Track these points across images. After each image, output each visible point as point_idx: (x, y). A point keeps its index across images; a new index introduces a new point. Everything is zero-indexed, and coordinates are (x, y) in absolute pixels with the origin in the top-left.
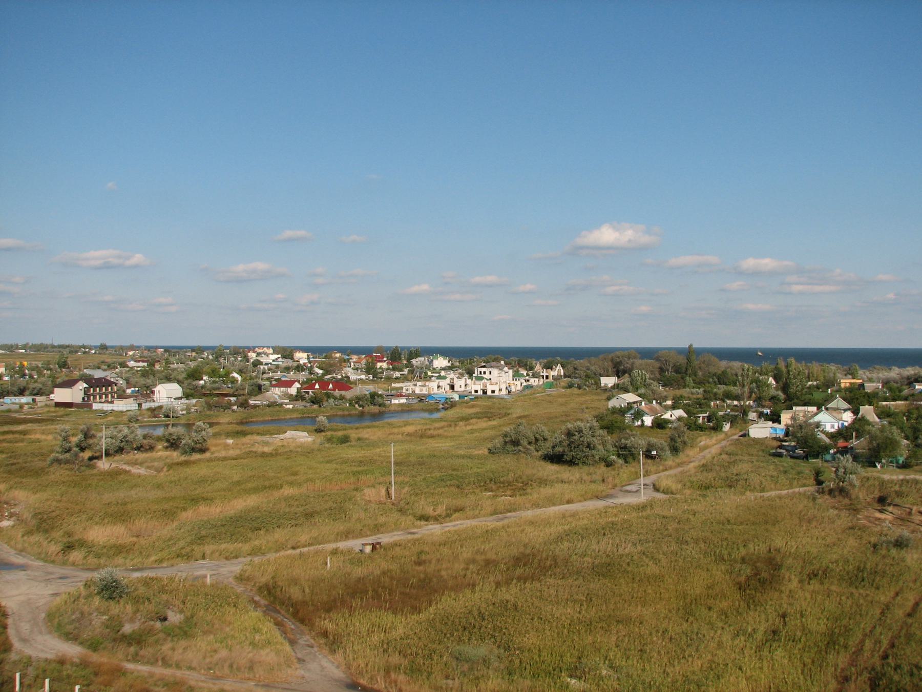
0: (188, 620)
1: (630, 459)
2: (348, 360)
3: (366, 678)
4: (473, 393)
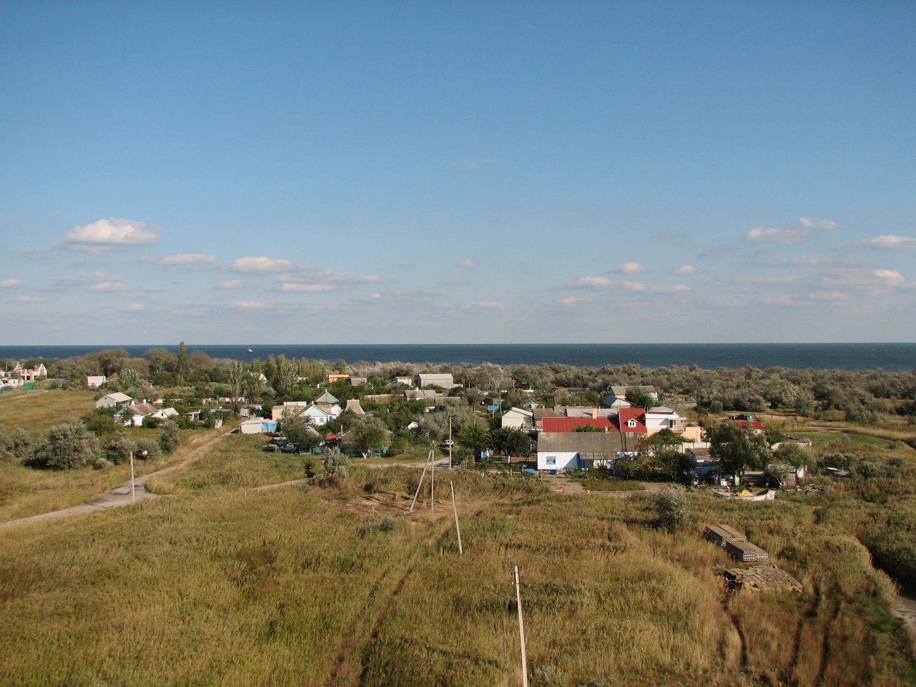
1: (121, 462)
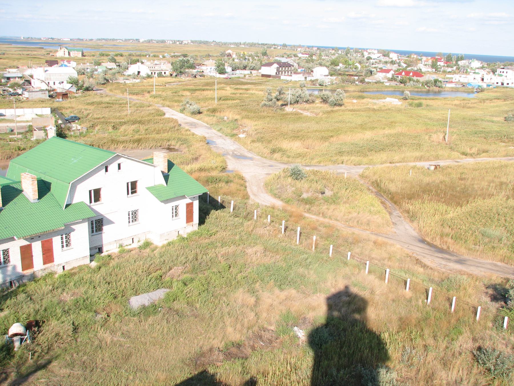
2: (421, 60)
3: (430, 238)
4: (495, 84)
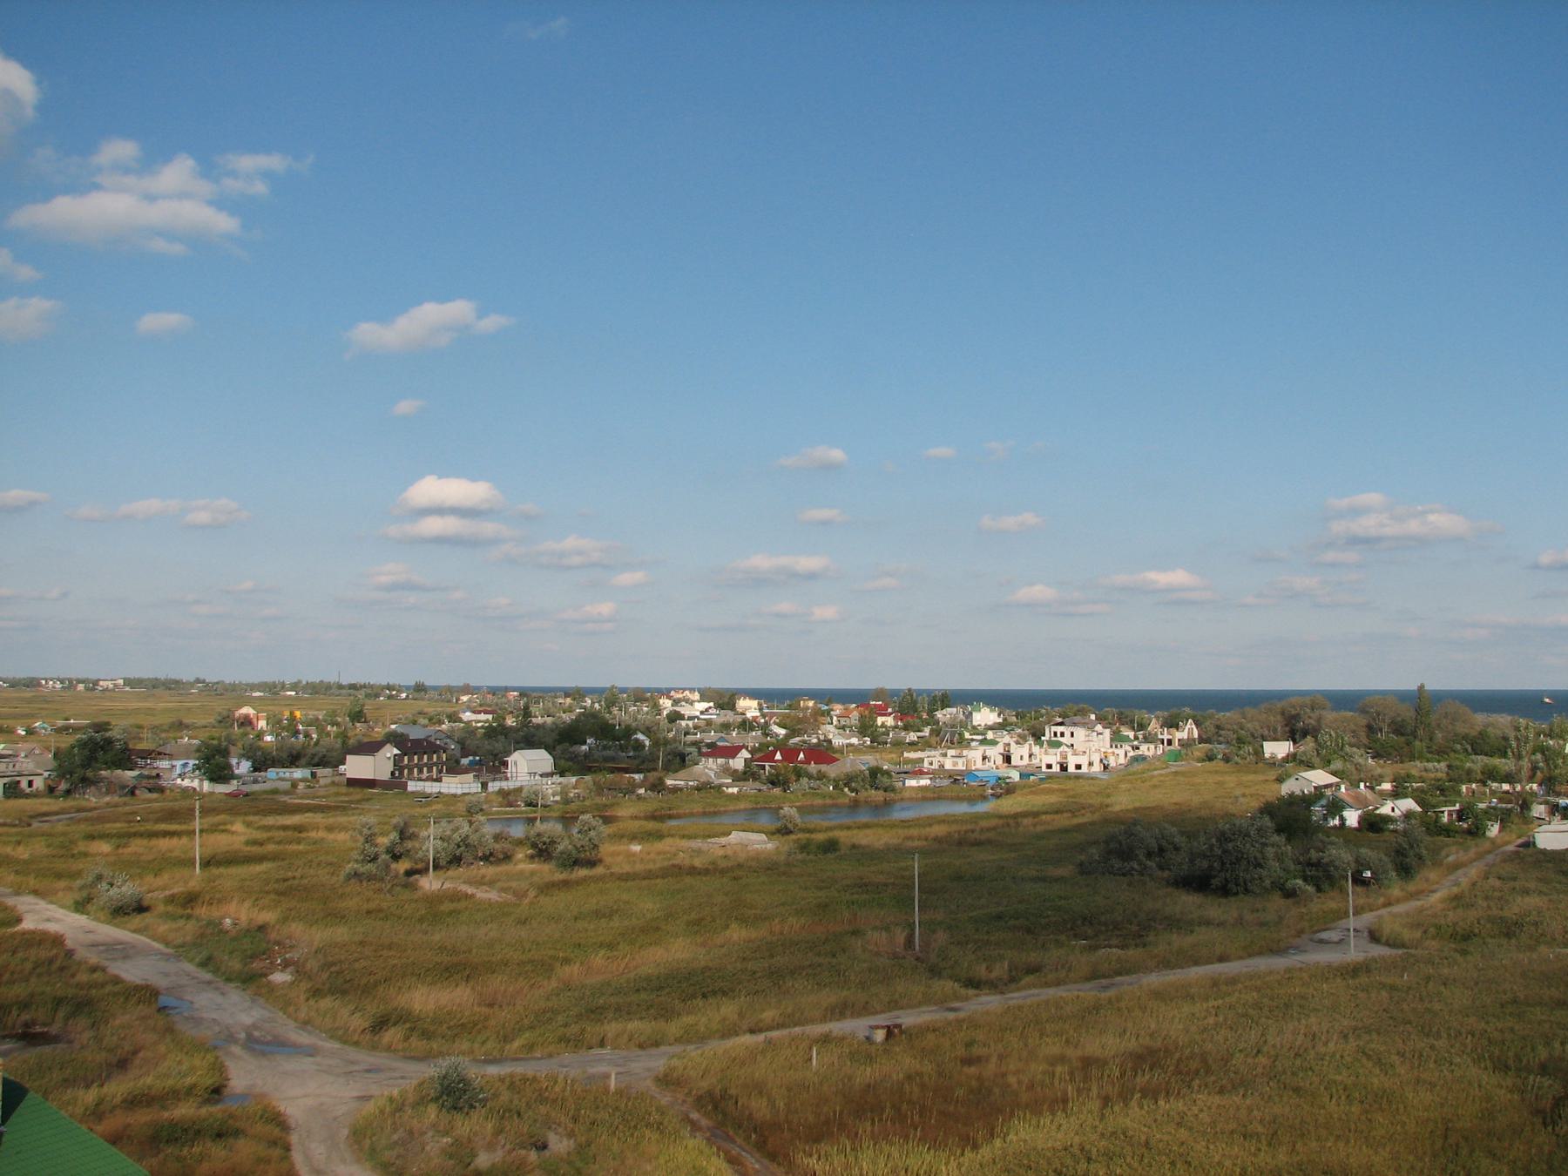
0: (581, 1149)
1: (1326, 886)
2: (828, 713)
4: (1044, 769)
